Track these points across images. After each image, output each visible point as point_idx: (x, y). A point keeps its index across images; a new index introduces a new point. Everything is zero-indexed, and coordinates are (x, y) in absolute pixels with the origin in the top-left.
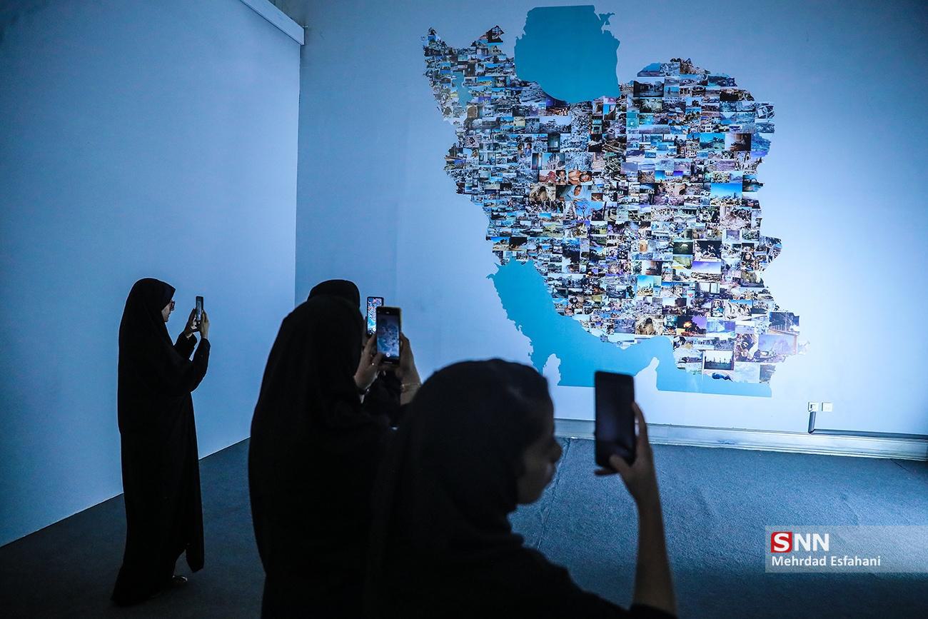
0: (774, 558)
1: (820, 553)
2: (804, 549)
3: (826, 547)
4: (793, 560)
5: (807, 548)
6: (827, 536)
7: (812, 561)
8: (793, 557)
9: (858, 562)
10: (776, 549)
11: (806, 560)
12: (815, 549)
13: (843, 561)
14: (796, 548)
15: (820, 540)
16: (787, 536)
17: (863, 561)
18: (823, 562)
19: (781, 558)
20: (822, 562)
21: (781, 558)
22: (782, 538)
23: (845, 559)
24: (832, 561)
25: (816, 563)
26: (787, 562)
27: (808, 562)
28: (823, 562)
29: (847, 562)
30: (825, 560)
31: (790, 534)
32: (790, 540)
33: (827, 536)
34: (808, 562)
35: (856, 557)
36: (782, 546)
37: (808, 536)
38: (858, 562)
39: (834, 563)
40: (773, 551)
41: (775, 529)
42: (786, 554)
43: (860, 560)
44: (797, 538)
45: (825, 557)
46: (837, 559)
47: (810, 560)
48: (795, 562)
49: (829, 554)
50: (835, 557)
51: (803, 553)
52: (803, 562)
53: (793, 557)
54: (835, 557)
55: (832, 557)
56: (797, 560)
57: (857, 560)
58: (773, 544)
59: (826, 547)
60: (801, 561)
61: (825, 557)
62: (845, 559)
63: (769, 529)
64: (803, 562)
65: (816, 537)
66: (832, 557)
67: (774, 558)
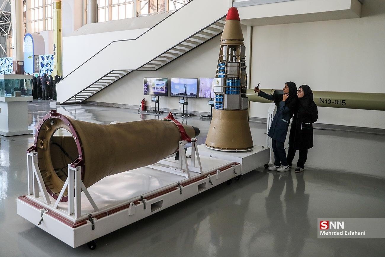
0: (321, 232)
1: (340, 230)
2: (334, 228)
3: (343, 227)
4: (329, 232)
5: (335, 227)
6: (343, 223)
7: (337, 233)
8: (329, 231)
9: (356, 233)
10: (322, 228)
11: (335, 232)
12: (338, 228)
13: (350, 233)
14: (330, 228)
15: (340, 225)
16: (326, 222)
17: (358, 233)
18: (341, 233)
19: (324, 232)
20: (341, 233)
21: (324, 232)
22: (324, 223)
23: (351, 232)
24: (345, 233)
25: (339, 234)
26: (326, 233)
27: (335, 233)
28: (341, 233)
29: (352, 233)
30: (342, 232)
31: (328, 222)
32: (328, 224)
33: (343, 223)
34: (335, 233)
35: (355, 231)
36: (324, 227)
37: (335, 222)
38: (356, 233)
39: (346, 234)
40: (321, 229)
41: (322, 219)
42: (326, 230)
43: (357, 232)
44: (331, 223)
45: (342, 231)
46: (347, 232)
47: (336, 233)
48: (330, 233)
49: (344, 230)
50: (347, 231)
51: (333, 230)
52: (333, 233)
53: (329, 231)
54: (347, 231)
55: (345, 231)
56: (331, 232)
57: (355, 232)
58: (321, 226)
59: (343, 227)
60: (332, 233)
61: (342, 231)
62: (351, 232)
63: (319, 220)
64: (333, 233)
65: (339, 223)
66: (345, 231)
67: (321, 232)
